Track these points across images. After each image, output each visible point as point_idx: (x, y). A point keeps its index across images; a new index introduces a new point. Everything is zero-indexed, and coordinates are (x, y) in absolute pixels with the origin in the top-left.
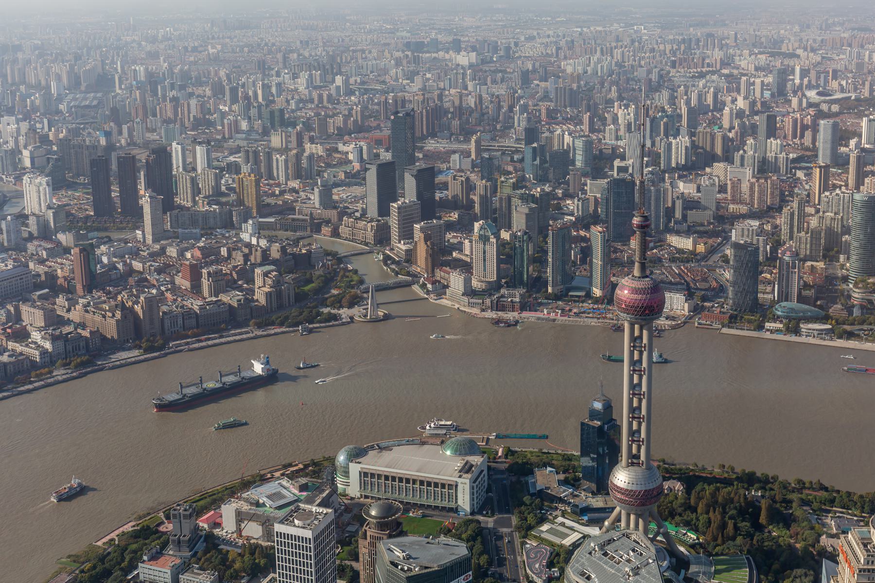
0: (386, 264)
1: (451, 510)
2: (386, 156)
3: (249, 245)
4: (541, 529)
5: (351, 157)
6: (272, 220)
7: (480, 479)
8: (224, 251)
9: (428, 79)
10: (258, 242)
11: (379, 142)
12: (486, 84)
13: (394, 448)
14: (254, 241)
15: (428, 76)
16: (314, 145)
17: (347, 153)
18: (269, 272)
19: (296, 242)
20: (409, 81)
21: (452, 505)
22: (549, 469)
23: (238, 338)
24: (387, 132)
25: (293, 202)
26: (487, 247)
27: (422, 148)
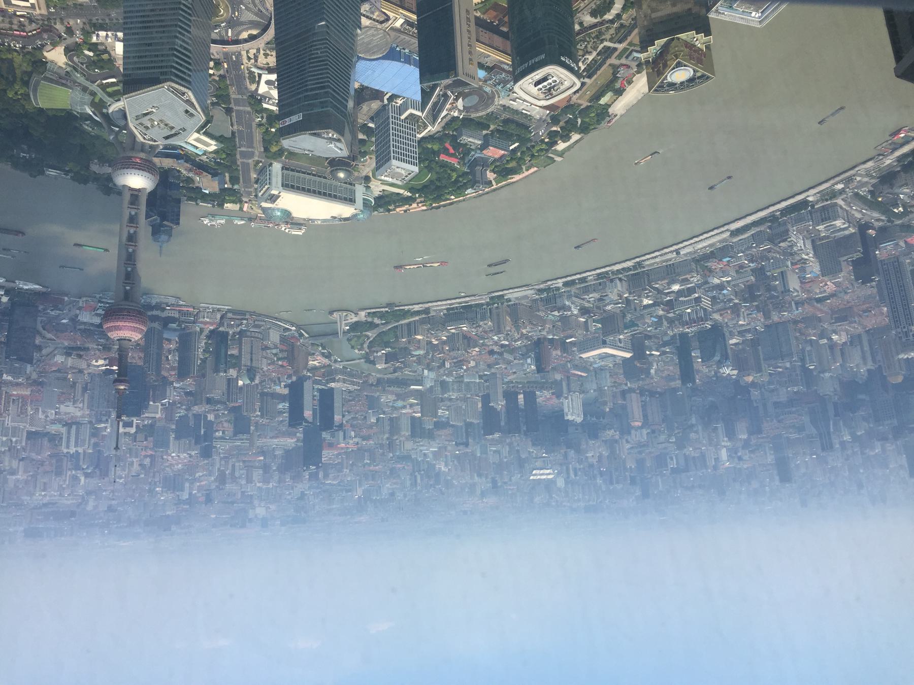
0: (329, 353)
1: (287, 169)
2: (325, 435)
3: (430, 370)
4: (216, 148)
5: (353, 434)
6: (412, 387)
7: (264, 189)
8: (447, 365)
9: (290, 494)
10: (423, 371)
11: (331, 446)
12: (242, 492)
13: (329, 217)
14: (426, 372)
15: (289, 497)
16: (380, 442)
17: (355, 437)
18: (416, 350)
19: (395, 371)
20: (306, 492)
21: (285, 172)
22: (207, 192)
23: (439, 303)
24: (324, 452)
25: (397, 400)
26: (249, 364)
27: (298, 441)
